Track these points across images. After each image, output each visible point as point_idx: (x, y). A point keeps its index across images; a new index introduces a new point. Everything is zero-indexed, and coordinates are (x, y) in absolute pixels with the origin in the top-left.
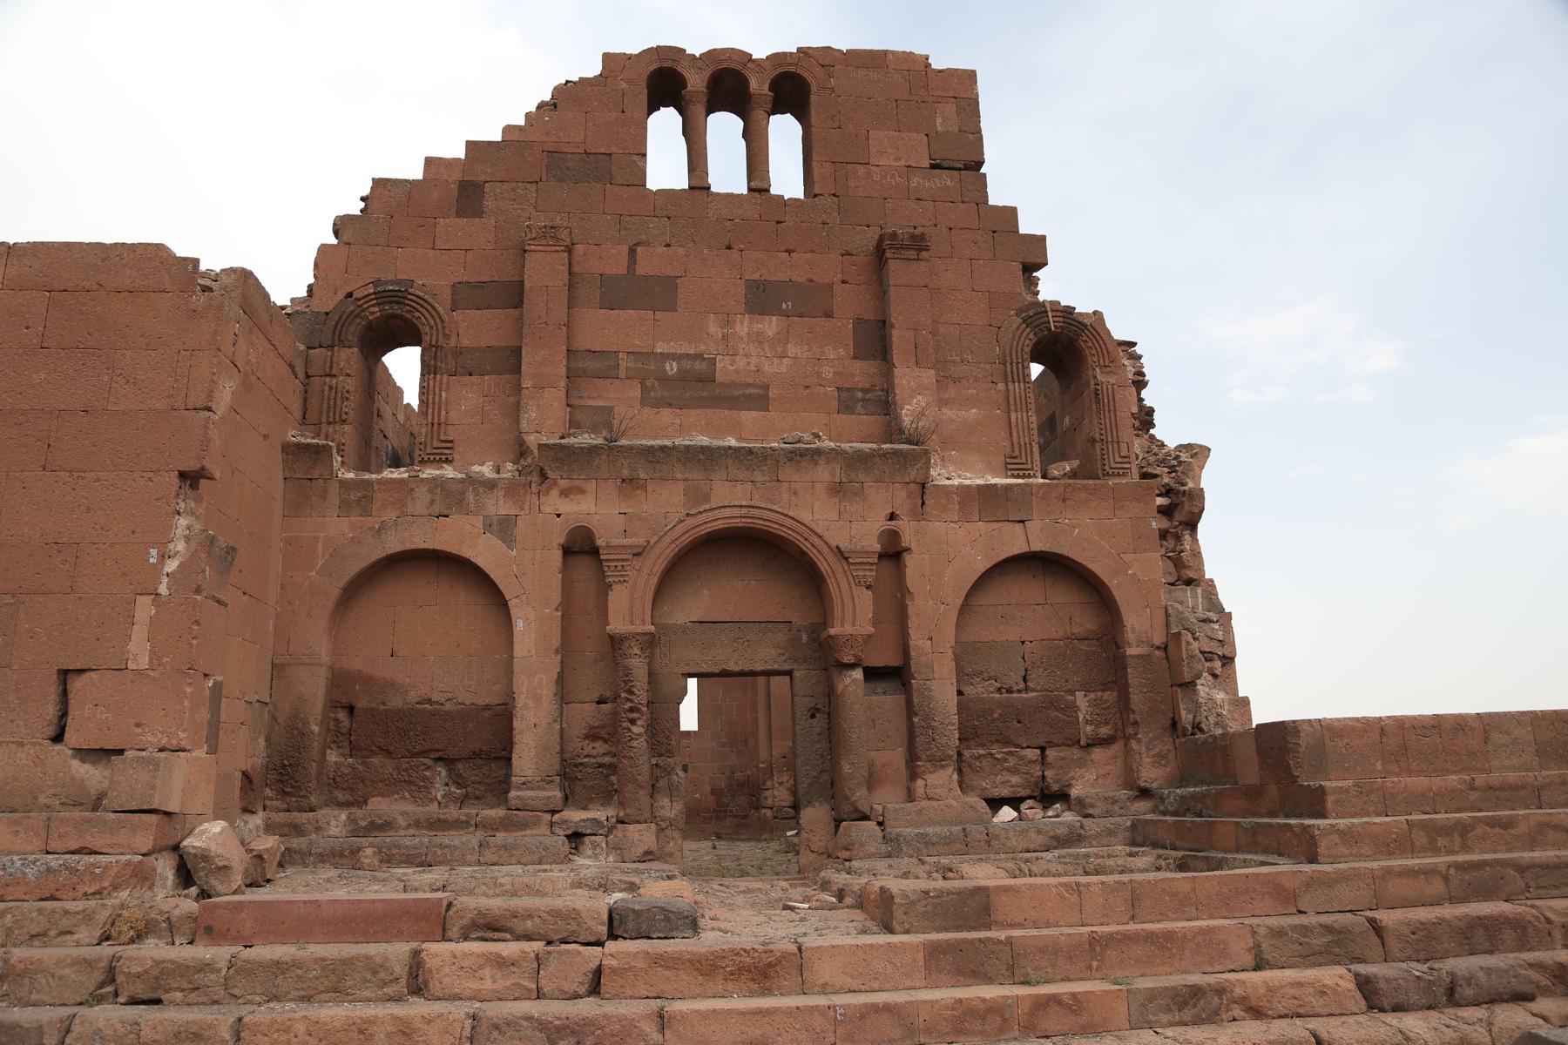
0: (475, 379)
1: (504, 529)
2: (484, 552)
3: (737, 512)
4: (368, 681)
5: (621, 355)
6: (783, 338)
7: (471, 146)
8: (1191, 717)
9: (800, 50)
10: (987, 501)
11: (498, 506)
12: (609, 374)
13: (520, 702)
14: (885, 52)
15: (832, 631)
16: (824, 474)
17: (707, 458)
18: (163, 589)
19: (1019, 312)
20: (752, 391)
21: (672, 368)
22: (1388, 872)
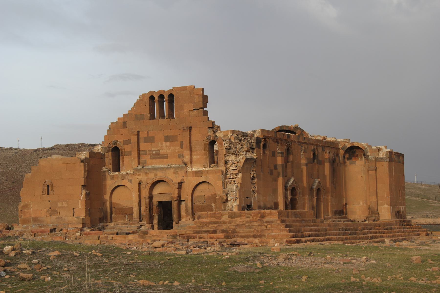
0: (127, 156)
1: (131, 181)
2: (128, 184)
3: (159, 178)
4: (117, 204)
5: (147, 151)
6: (170, 146)
7: (124, 115)
8: (224, 208)
9: (173, 88)
10: (198, 173)
11: (130, 178)
12: (145, 154)
13: (134, 207)
14: (186, 87)
15: (172, 196)
16: (172, 170)
17: (156, 169)
18: (82, 199)
19: (207, 137)
20: (165, 155)
21: (154, 152)
22: (187, 231)
